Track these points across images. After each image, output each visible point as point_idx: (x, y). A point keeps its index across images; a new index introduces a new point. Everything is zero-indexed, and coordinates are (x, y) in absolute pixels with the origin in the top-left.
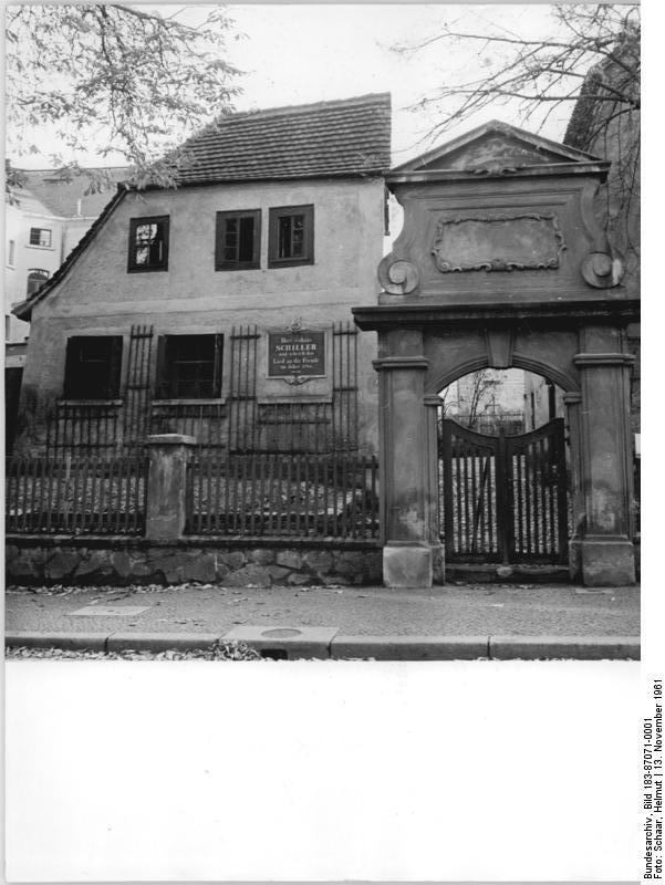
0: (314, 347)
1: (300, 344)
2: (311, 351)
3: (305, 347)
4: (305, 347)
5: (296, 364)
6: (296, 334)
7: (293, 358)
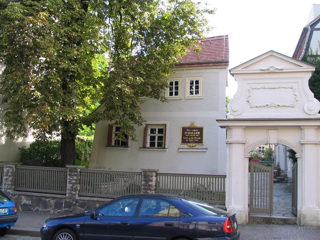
0: (199, 133)
1: (194, 132)
2: (198, 135)
4: (195, 133)
6: (191, 129)
7: (191, 137)
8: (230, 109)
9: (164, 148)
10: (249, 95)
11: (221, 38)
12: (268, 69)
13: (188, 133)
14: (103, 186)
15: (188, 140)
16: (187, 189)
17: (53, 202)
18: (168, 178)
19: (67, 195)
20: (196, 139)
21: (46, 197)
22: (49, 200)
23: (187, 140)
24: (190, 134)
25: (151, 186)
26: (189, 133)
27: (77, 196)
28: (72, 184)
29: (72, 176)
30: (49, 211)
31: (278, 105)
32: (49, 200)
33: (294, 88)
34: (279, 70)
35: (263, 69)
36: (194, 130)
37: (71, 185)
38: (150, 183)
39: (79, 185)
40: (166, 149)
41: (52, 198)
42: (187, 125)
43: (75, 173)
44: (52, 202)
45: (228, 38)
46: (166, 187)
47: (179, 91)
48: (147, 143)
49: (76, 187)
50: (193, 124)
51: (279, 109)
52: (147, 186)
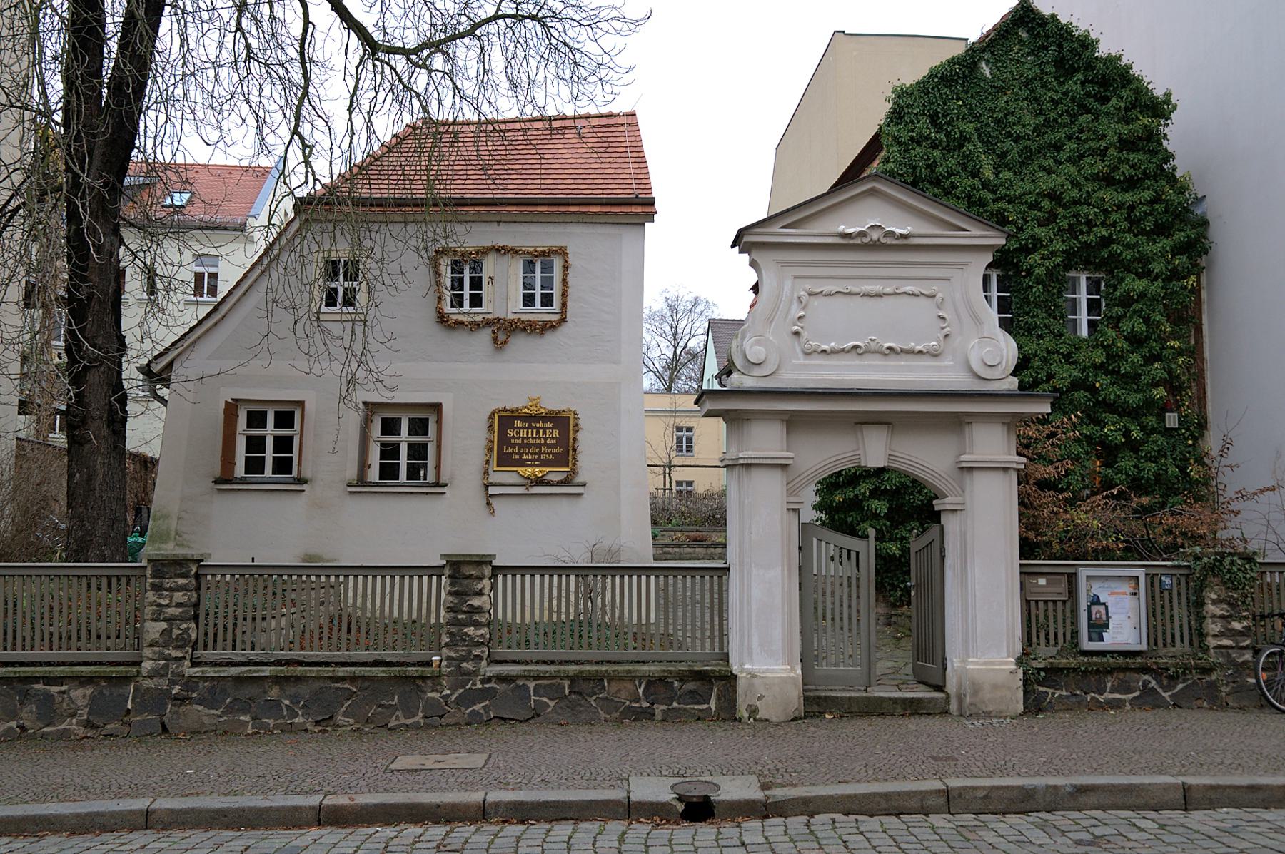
0: (556, 433)
3: (544, 433)
4: (544, 433)
5: (532, 454)
8: (741, 357)
9: (301, 481)
10: (802, 313)
11: (612, 121)
12: (862, 234)
13: (519, 433)
14: (273, 622)
15: (521, 455)
16: (626, 620)
17: (84, 697)
18: (702, 584)
19: (147, 665)
20: (549, 454)
21: (49, 681)
22: (65, 688)
23: (517, 457)
24: (527, 438)
25: (479, 610)
26: (523, 433)
27: (187, 663)
28: (164, 620)
29: (166, 593)
30: (65, 735)
31: (890, 348)
32: (65, 688)
33: (940, 295)
34: (897, 239)
35: (849, 231)
36: (541, 424)
37: (164, 625)
38: (476, 602)
39: (193, 625)
40: (445, 485)
41: (76, 683)
42: (516, 401)
43: (181, 581)
44: (80, 695)
45: (636, 124)
46: (563, 617)
47: (486, 292)
48: (369, 467)
49: (186, 631)
50: (535, 402)
51: (893, 362)
52: (465, 612)
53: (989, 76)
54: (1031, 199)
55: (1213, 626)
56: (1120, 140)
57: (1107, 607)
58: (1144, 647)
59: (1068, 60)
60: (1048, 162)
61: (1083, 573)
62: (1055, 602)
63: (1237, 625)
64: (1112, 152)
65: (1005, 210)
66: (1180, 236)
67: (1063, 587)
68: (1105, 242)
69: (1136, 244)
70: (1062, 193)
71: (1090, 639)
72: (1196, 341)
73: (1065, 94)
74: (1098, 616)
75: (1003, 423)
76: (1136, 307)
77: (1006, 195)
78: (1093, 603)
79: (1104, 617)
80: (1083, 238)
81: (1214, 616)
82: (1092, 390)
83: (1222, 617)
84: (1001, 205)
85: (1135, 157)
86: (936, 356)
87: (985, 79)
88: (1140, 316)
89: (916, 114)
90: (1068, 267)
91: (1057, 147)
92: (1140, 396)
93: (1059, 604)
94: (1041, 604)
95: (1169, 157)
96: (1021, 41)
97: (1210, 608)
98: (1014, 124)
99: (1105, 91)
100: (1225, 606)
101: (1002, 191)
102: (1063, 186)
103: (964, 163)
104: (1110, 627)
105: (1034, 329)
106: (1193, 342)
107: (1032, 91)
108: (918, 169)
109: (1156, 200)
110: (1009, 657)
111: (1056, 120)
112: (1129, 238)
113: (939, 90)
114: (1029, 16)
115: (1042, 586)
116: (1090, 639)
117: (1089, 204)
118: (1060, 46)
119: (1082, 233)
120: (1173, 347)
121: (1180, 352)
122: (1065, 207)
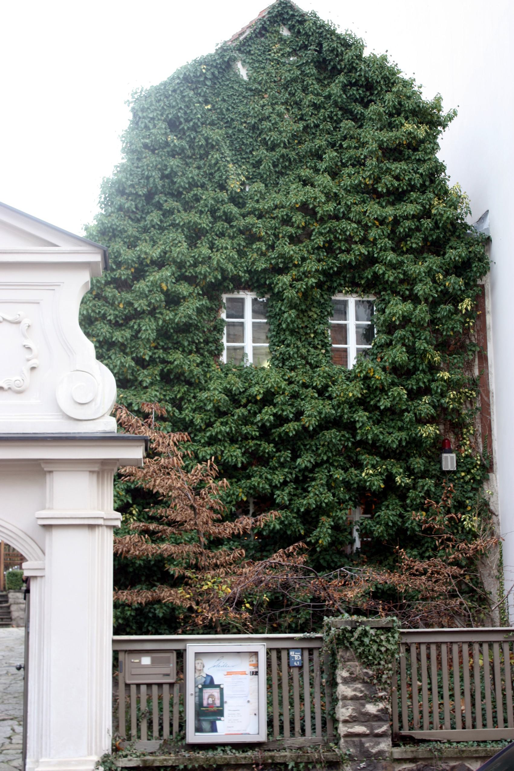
33: (26, 322)
53: (246, 78)
54: (280, 213)
55: (343, 710)
56: (380, 147)
57: (222, 690)
58: (262, 737)
59: (330, 61)
60: (305, 172)
61: (191, 649)
62: (160, 685)
63: (371, 708)
64: (372, 162)
65: (253, 225)
66: (452, 254)
67: (172, 666)
68: (371, 260)
69: (401, 263)
70: (315, 207)
71: (199, 729)
72: (480, 371)
73: (329, 97)
74: (210, 701)
75: (92, 472)
76: (399, 333)
77: (255, 209)
78: (205, 686)
79: (218, 703)
80: (343, 257)
81: (345, 698)
82: (351, 427)
83: (354, 698)
84: (250, 220)
85: (397, 167)
86: (19, 392)
87: (238, 80)
88: (404, 345)
89: (153, 119)
90: (332, 290)
91: (318, 155)
92: (403, 435)
93: (166, 688)
94: (143, 688)
95: (439, 168)
96: (281, 40)
97: (343, 690)
98: (270, 130)
99: (372, 94)
100: (359, 686)
101: (250, 205)
102: (315, 198)
103: (211, 174)
104: (226, 713)
105: (287, 359)
106: (476, 372)
107: (292, 95)
108: (151, 180)
109: (426, 213)
110: (90, 754)
111: (317, 126)
112: (391, 256)
113: (182, 92)
114: (287, 13)
115: (146, 667)
116: (199, 729)
117: (349, 219)
118: (320, 45)
119: (342, 251)
120: (442, 379)
121: (450, 384)
122: (322, 221)
